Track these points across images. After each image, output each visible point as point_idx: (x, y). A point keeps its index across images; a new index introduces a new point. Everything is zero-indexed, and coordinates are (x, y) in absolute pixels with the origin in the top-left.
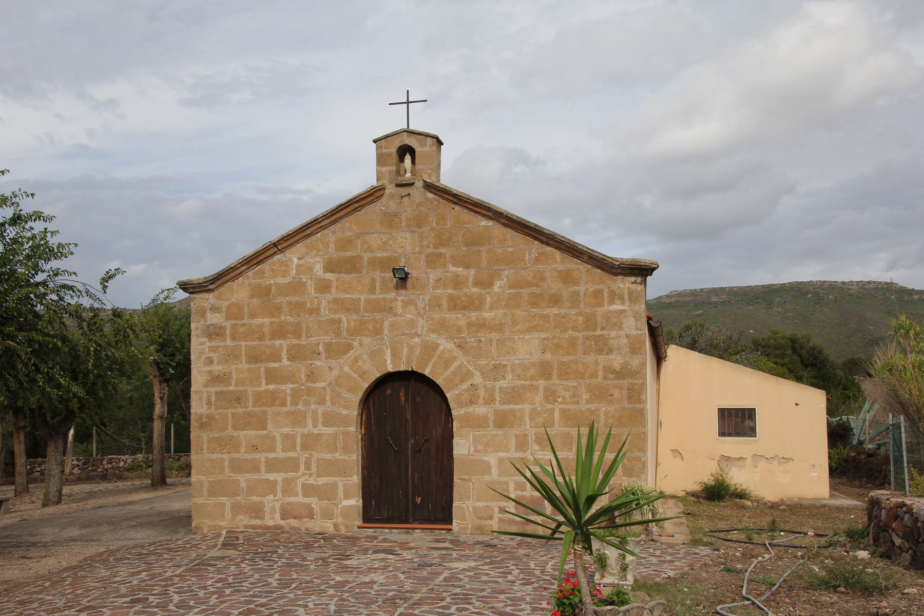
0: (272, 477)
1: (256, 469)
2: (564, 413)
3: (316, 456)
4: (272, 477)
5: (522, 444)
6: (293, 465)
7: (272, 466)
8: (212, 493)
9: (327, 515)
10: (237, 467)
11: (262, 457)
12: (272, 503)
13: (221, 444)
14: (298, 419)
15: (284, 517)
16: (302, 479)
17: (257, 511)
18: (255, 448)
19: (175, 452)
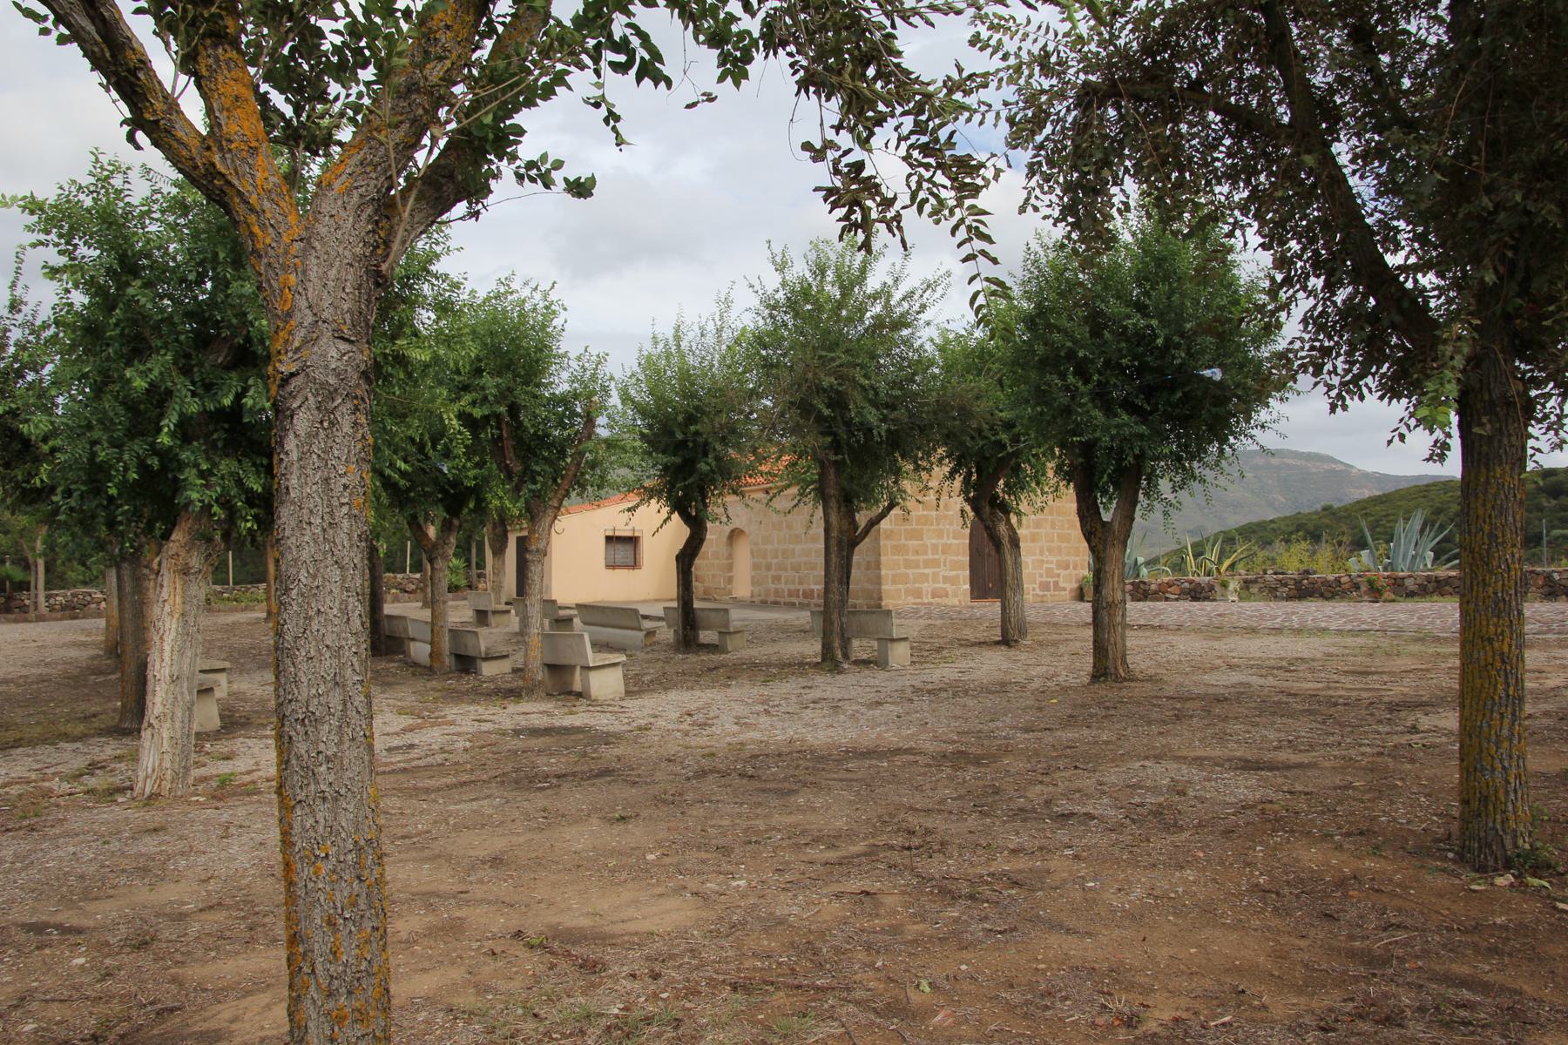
0: (926, 571)
1: (917, 566)
2: (1059, 535)
3: (950, 558)
4: (926, 571)
5: (1041, 553)
6: (936, 564)
7: (927, 564)
8: (894, 582)
9: (956, 595)
10: (908, 565)
11: (921, 558)
12: (927, 587)
13: (898, 550)
14: (940, 534)
15: (933, 596)
16: (943, 572)
17: (918, 593)
18: (917, 553)
19: (235, 583)
